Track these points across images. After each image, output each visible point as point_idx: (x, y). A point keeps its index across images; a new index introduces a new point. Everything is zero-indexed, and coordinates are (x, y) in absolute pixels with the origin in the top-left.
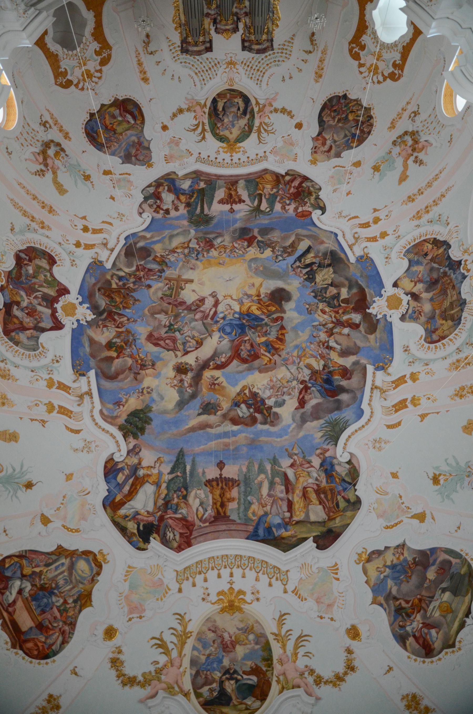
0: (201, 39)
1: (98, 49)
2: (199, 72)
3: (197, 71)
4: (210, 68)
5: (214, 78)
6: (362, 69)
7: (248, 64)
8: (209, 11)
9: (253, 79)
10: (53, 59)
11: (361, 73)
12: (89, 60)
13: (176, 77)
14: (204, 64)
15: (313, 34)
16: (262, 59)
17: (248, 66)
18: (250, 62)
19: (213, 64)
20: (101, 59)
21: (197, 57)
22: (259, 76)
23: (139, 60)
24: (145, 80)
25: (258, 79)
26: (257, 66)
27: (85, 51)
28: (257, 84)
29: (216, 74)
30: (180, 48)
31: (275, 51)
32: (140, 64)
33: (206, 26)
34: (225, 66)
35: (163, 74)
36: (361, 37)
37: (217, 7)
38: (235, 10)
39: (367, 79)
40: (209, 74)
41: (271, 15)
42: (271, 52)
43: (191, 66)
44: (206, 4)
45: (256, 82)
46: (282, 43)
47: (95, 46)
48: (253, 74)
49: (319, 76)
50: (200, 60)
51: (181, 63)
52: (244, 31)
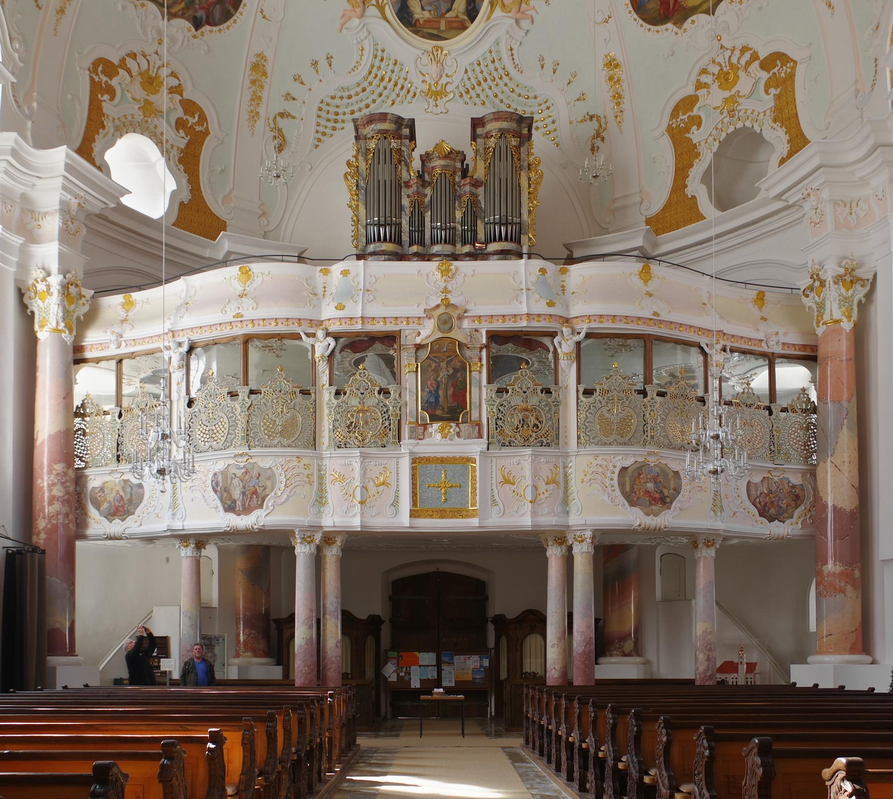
0: (492, 142)
1: (695, 127)
2: (501, 78)
3: (505, 79)
4: (479, 84)
5: (471, 64)
6: (174, 82)
7: (403, 93)
8: (474, 190)
9: (392, 62)
10: (786, 114)
11: (173, 74)
12: (715, 108)
13: (549, 67)
14: (489, 92)
15: (280, 149)
16: (374, 101)
17: (402, 88)
18: (398, 95)
19: (472, 92)
20: (692, 110)
21: (504, 108)
22: (379, 68)
23: (618, 104)
24: (612, 64)
25: (382, 60)
26: (385, 88)
27: (719, 126)
28: (383, 51)
29: (466, 71)
30: (534, 125)
31: (349, 117)
32: (618, 97)
33: (481, 165)
34: (449, 88)
35: (574, 76)
36: (187, 144)
37: (460, 197)
38: (428, 191)
39: (159, 63)
40: (482, 72)
41: (362, 183)
42: (357, 115)
43: (517, 90)
44: (479, 202)
45: (385, 55)
46: (337, 132)
47: (696, 135)
48: (393, 71)
49: (259, 68)
50: (497, 101)
51: (535, 97)
52: (410, 156)
